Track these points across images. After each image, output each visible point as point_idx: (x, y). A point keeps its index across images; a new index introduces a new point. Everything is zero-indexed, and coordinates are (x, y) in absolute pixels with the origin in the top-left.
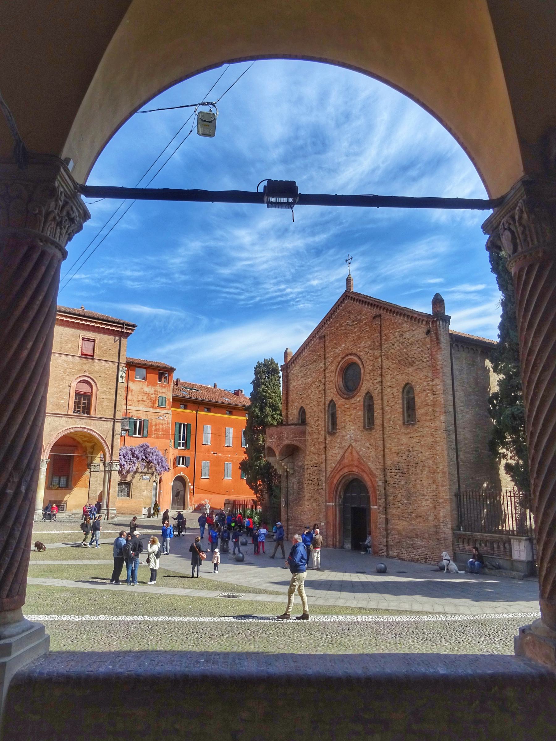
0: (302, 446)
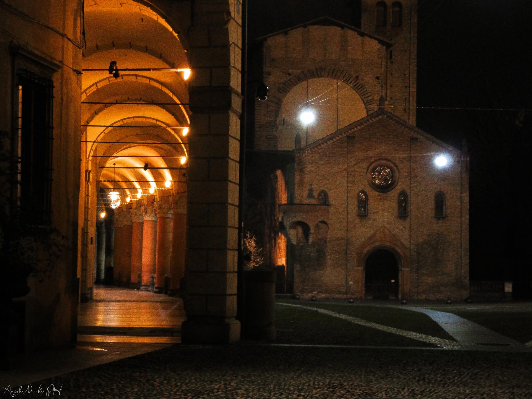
0: (327, 222)
